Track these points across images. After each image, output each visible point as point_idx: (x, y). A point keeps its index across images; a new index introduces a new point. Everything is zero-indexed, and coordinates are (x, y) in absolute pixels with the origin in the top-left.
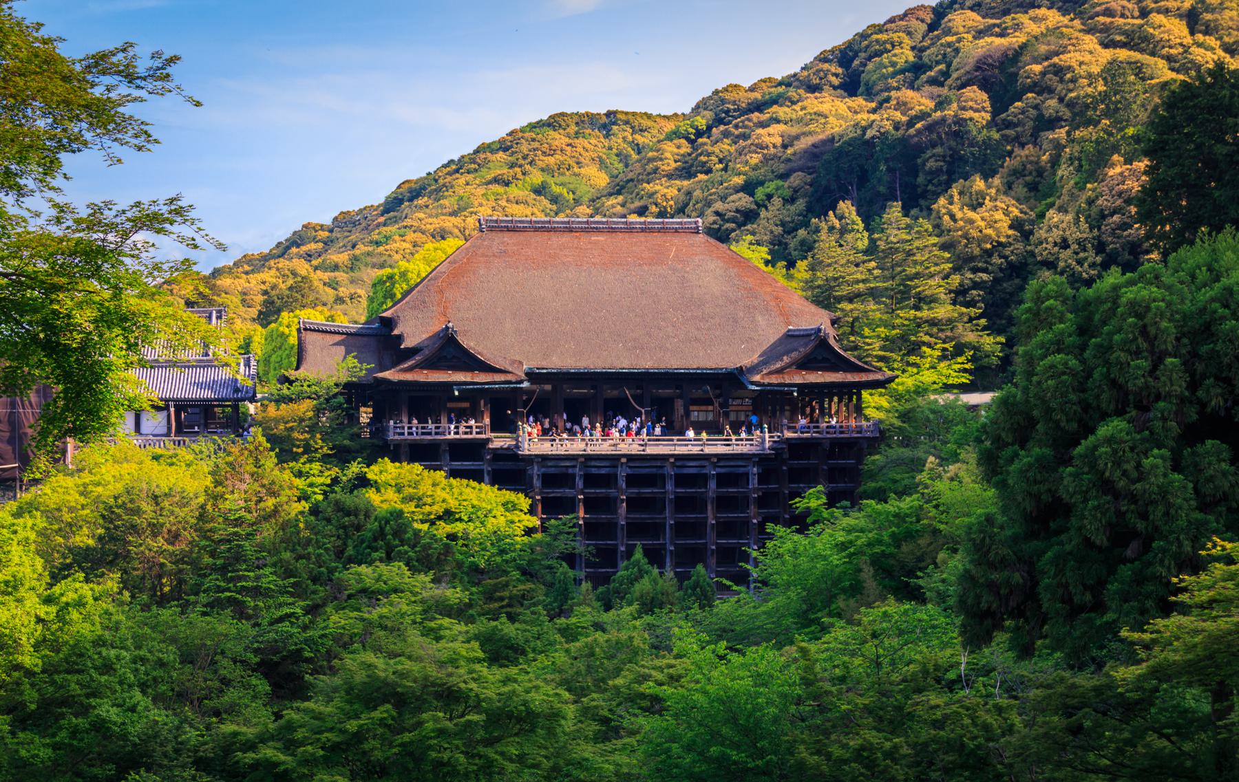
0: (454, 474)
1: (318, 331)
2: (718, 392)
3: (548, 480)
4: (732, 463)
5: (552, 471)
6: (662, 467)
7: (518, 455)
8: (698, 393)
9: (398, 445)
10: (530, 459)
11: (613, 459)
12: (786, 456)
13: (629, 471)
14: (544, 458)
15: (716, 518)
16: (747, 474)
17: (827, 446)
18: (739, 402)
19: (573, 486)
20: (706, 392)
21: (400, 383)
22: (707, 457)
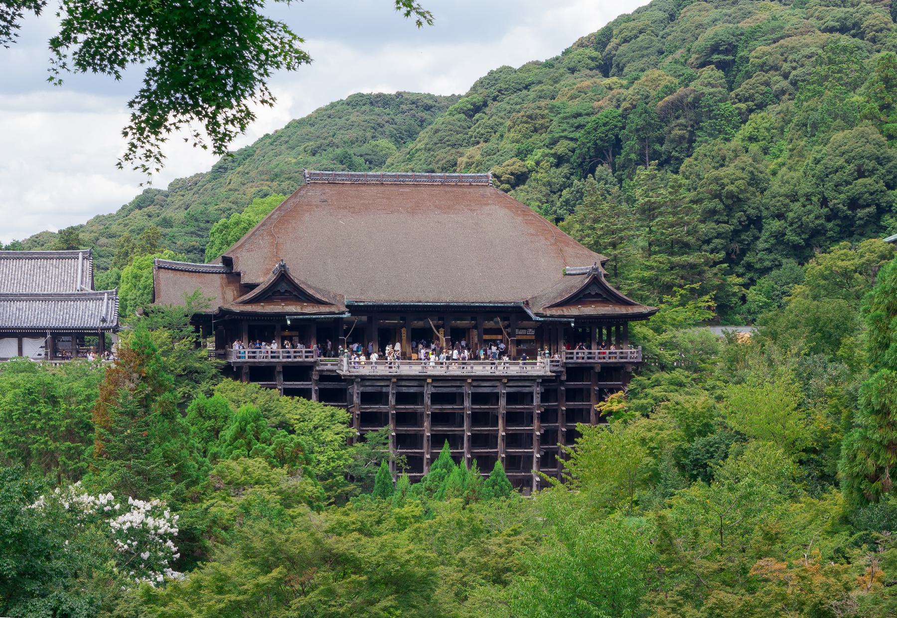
0: (288, 392)
1: (171, 269)
3: (366, 398)
4: (520, 384)
5: (369, 390)
6: (461, 387)
8: (489, 324)
9: (240, 367)
10: (350, 380)
11: (420, 380)
12: (564, 378)
13: (434, 390)
14: (363, 378)
15: (505, 430)
16: (531, 394)
17: (598, 369)
18: (524, 332)
19: (387, 404)
20: (497, 323)
21: (242, 313)
22: (498, 379)
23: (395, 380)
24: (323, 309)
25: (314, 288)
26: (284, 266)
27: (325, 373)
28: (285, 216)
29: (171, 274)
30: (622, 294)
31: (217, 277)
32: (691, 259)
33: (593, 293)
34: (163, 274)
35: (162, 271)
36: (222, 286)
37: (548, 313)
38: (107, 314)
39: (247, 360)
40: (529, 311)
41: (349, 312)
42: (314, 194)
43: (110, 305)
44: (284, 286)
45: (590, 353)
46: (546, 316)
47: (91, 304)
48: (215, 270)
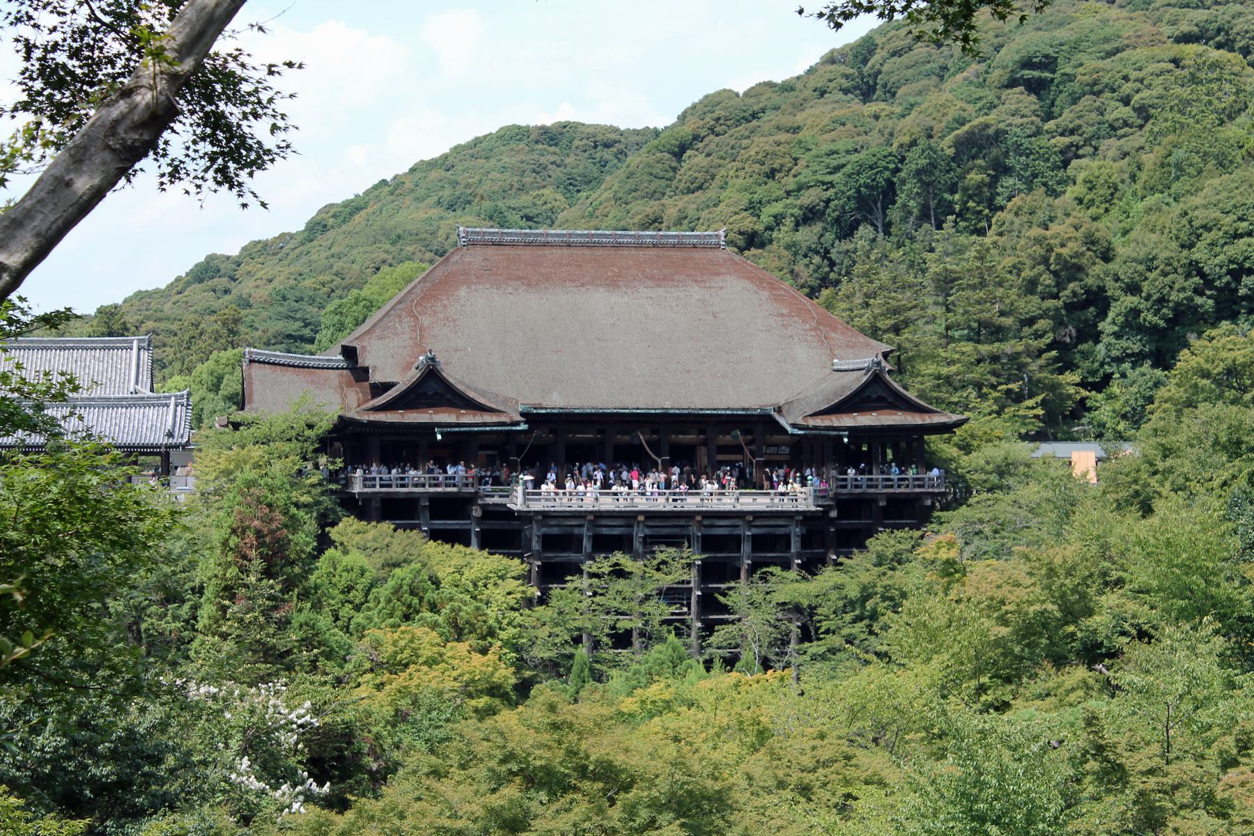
0: (435, 535)
1: (269, 363)
2: (749, 437)
3: (549, 542)
4: (771, 523)
5: (555, 531)
7: (511, 512)
8: (727, 439)
10: (527, 517)
11: (629, 517)
12: (834, 514)
13: (647, 531)
14: (546, 516)
16: (787, 537)
18: (773, 450)
19: (579, 549)
21: (371, 424)
23: (592, 517)
24: (488, 418)
25: (475, 390)
26: (433, 359)
27: (491, 508)
28: (435, 289)
30: (912, 395)
31: (333, 374)
32: (1010, 347)
33: (874, 396)
34: (257, 371)
37: (812, 422)
38: (174, 426)
39: (378, 489)
40: (782, 421)
41: (525, 423)
42: (475, 258)
44: (432, 387)
45: (871, 480)
46: (807, 428)
47: (151, 412)
48: (331, 364)
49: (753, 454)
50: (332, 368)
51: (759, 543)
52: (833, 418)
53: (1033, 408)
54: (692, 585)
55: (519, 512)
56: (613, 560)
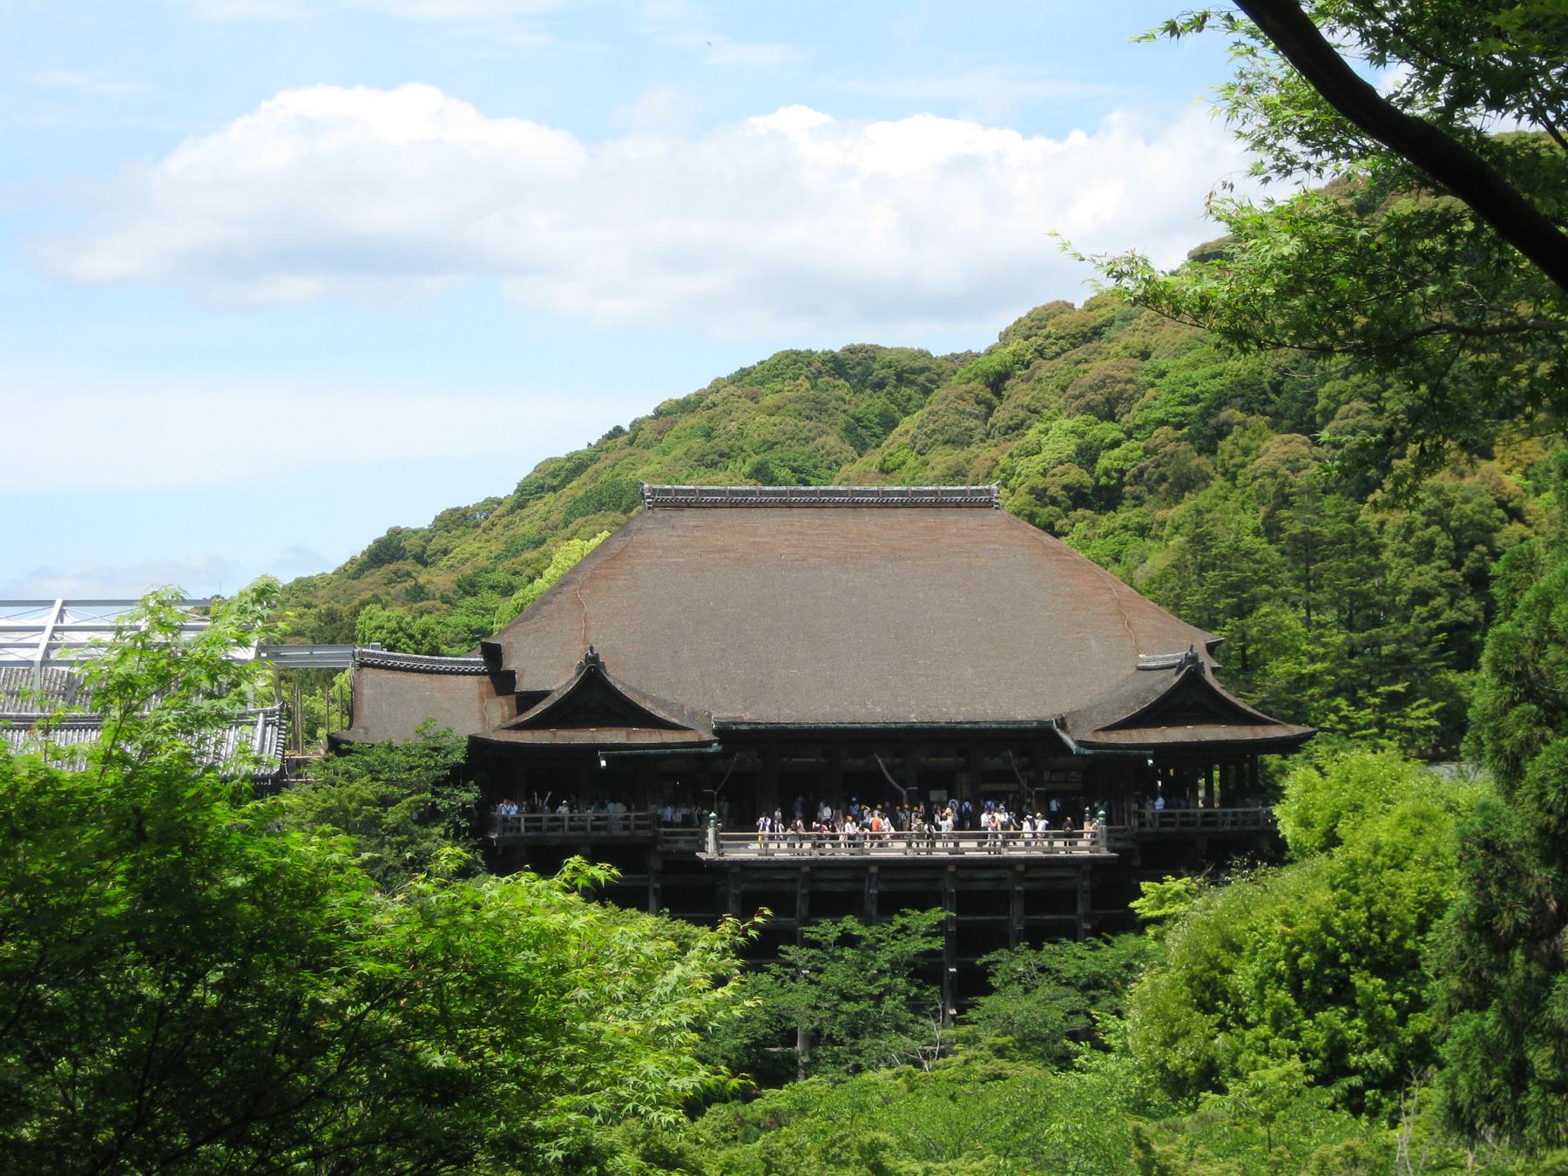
2: (1025, 759)
4: (1050, 874)
8: (995, 763)
10: (721, 869)
11: (859, 869)
12: (1136, 862)
13: (883, 887)
19: (792, 914)
22: (1010, 863)
23: (806, 869)
25: (652, 700)
29: (383, 674)
35: (366, 670)
36: (482, 700)
37: (1104, 738)
41: (720, 743)
43: (268, 736)
44: (595, 696)
45: (1186, 815)
49: (1031, 784)
50: (470, 673)
51: (1033, 901)
52: (1134, 732)
53: (1425, 719)
54: (945, 958)
55: (708, 861)
56: (841, 926)
